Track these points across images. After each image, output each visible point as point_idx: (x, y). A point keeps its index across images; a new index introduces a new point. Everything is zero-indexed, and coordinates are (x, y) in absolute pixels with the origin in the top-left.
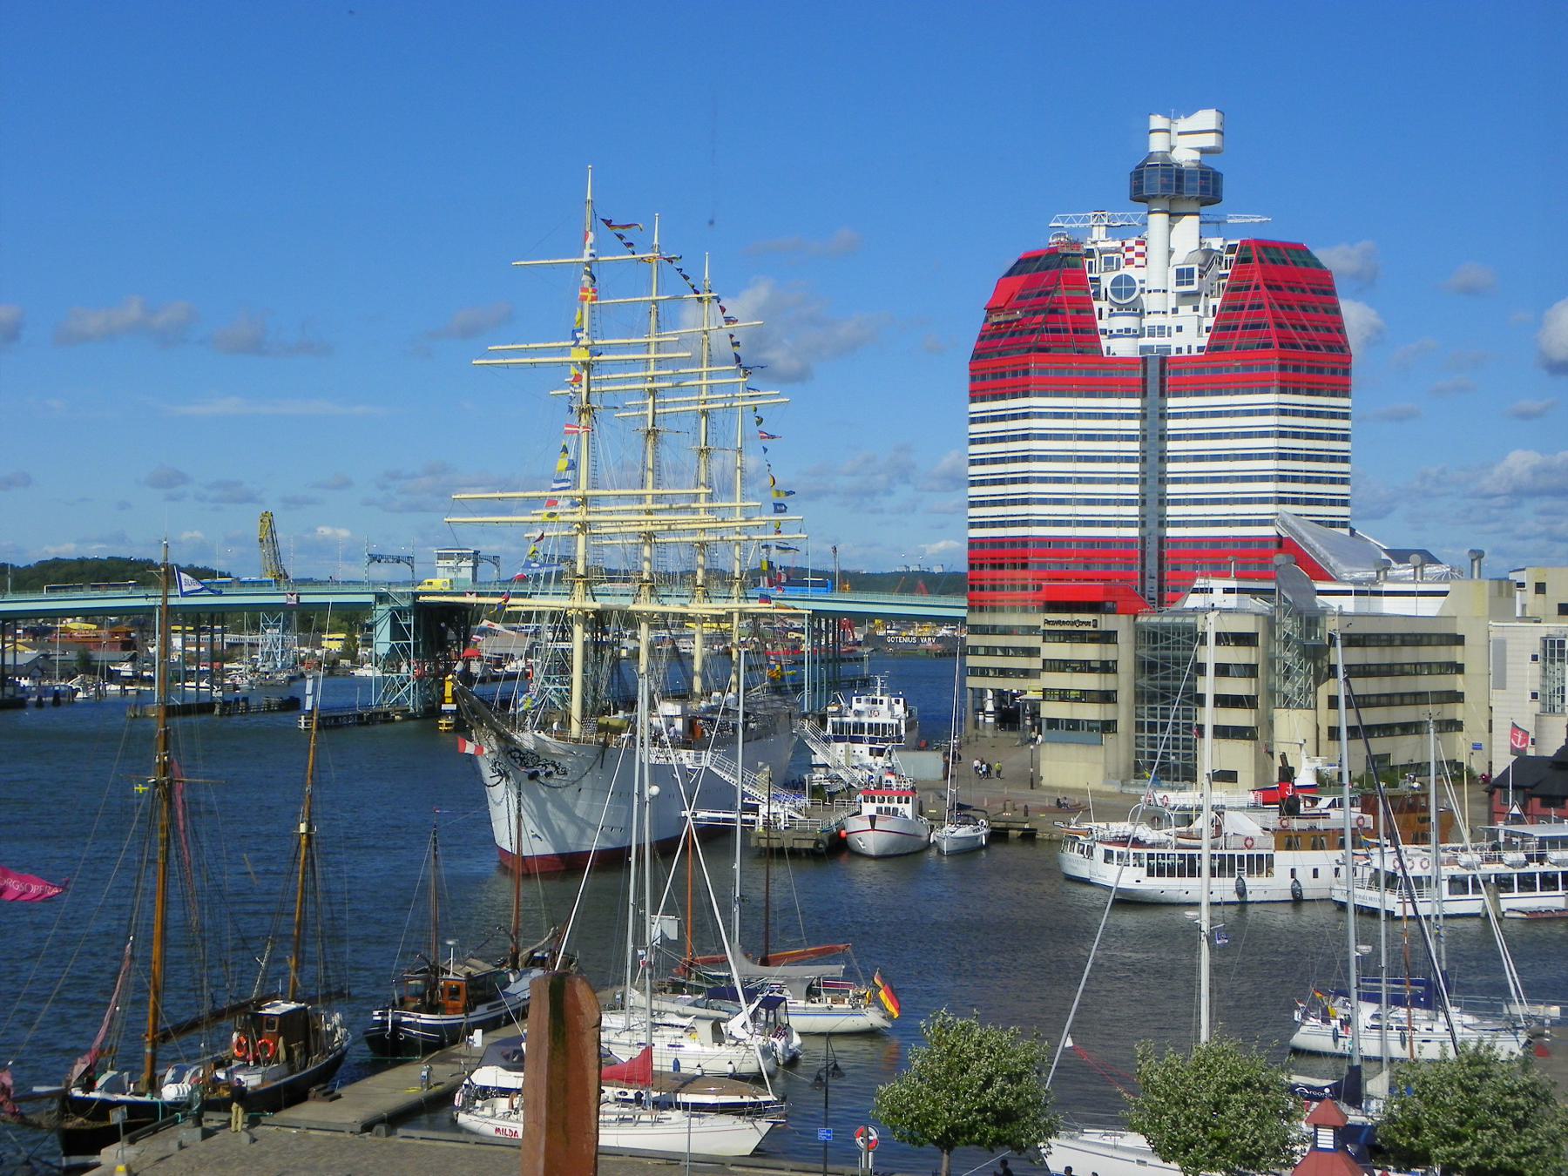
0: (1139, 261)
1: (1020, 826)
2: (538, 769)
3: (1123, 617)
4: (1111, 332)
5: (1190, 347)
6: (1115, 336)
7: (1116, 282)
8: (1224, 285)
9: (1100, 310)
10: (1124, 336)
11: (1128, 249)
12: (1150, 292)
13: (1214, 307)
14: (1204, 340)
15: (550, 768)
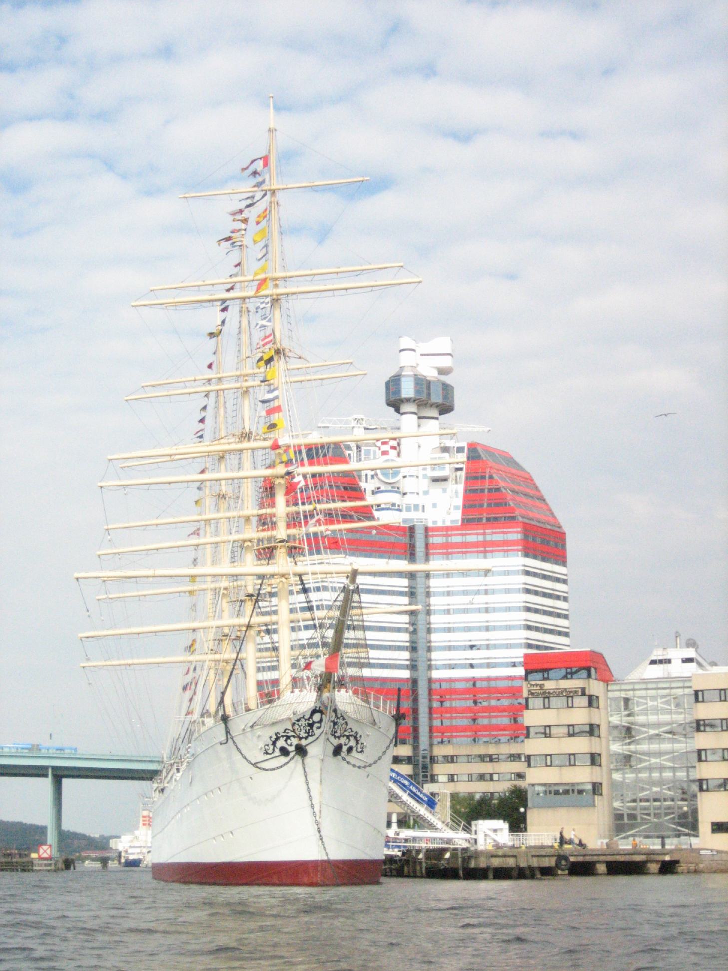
0: (393, 453)
2: (343, 740)
4: (379, 506)
5: (444, 522)
6: (383, 509)
10: (391, 510)
15: (352, 743)
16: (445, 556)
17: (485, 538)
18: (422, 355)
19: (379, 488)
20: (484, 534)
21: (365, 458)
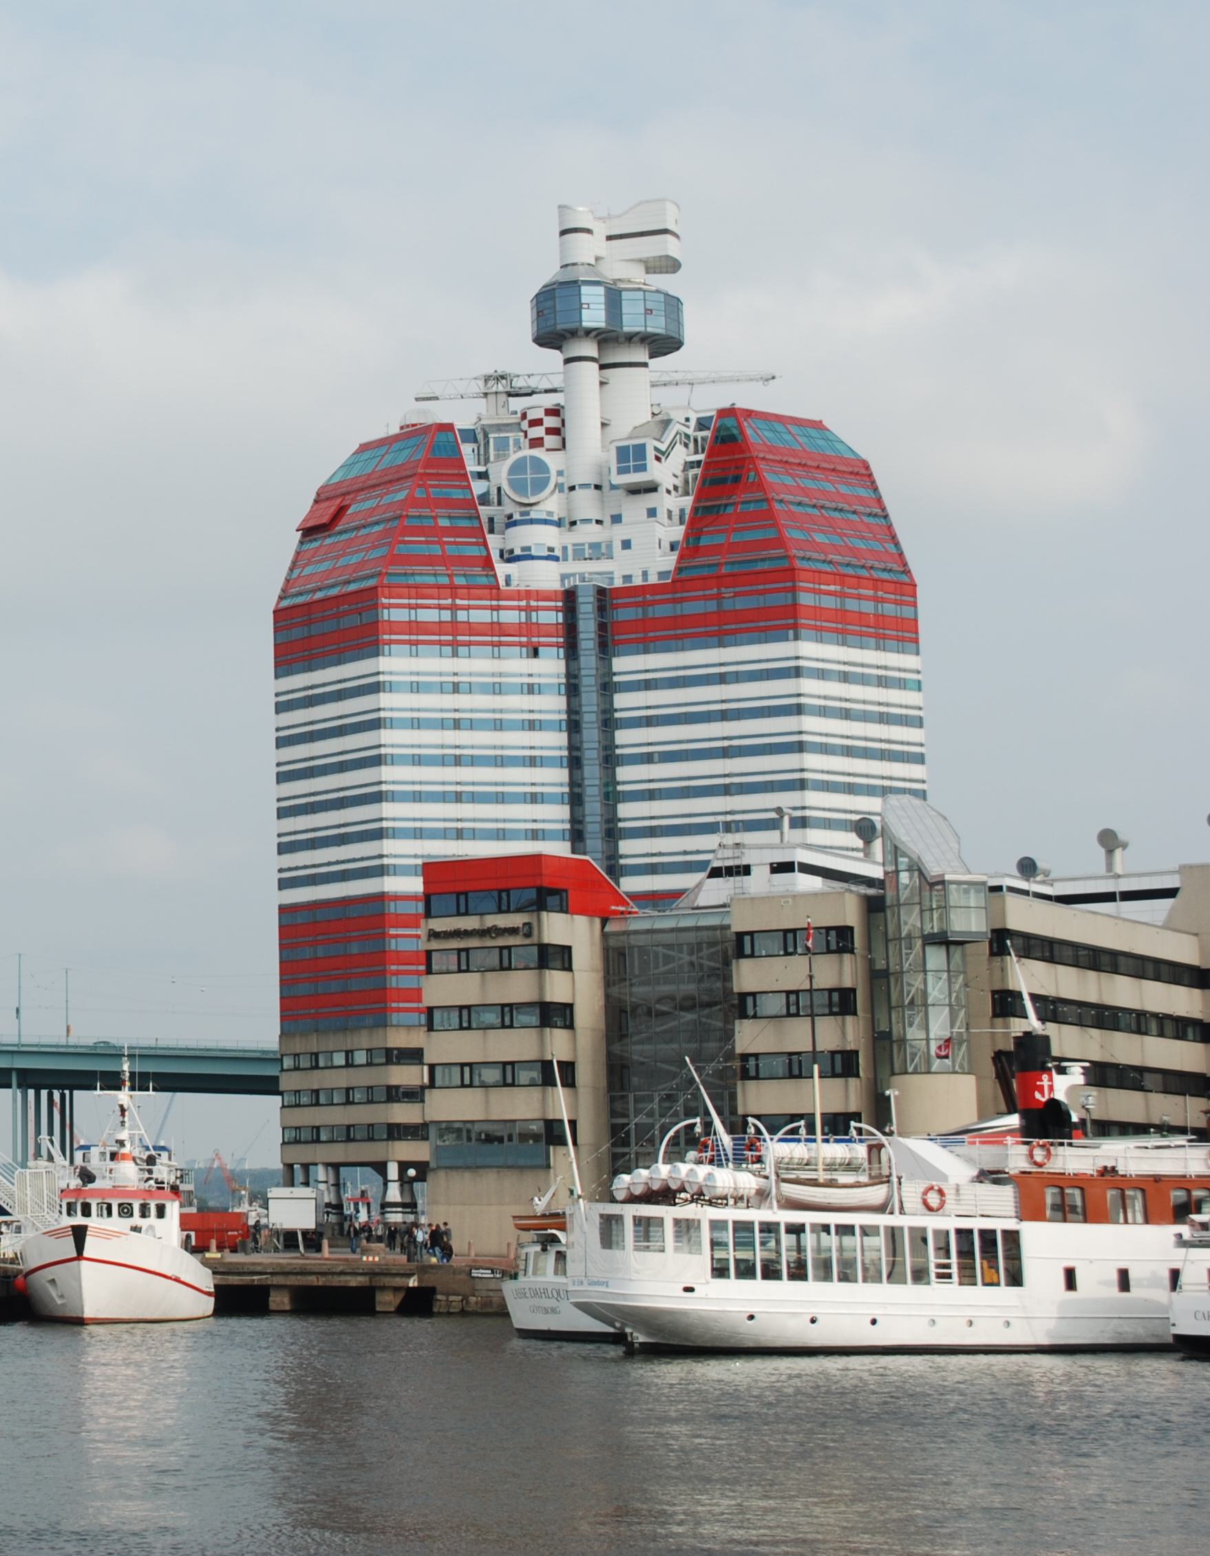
0: (550, 441)
1: (398, 1281)
3: (581, 921)
4: (512, 551)
5: (645, 574)
7: (518, 467)
8: (695, 477)
9: (491, 520)
11: (536, 423)
12: (572, 488)
13: (682, 511)
14: (669, 562)
16: (641, 646)
17: (719, 605)
18: (609, 238)
19: (510, 516)
20: (718, 597)
21: (498, 457)
